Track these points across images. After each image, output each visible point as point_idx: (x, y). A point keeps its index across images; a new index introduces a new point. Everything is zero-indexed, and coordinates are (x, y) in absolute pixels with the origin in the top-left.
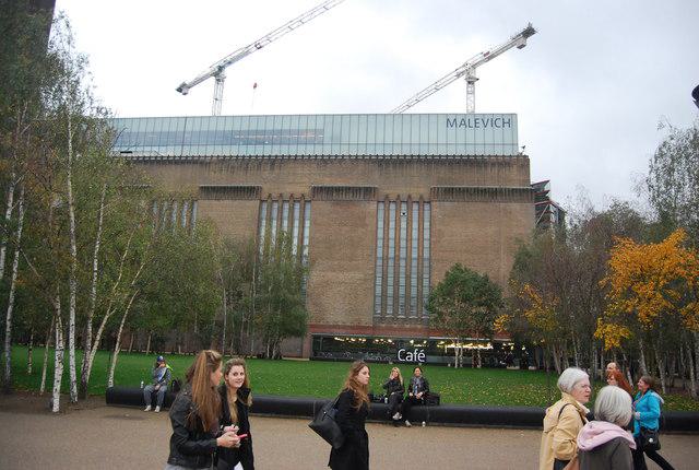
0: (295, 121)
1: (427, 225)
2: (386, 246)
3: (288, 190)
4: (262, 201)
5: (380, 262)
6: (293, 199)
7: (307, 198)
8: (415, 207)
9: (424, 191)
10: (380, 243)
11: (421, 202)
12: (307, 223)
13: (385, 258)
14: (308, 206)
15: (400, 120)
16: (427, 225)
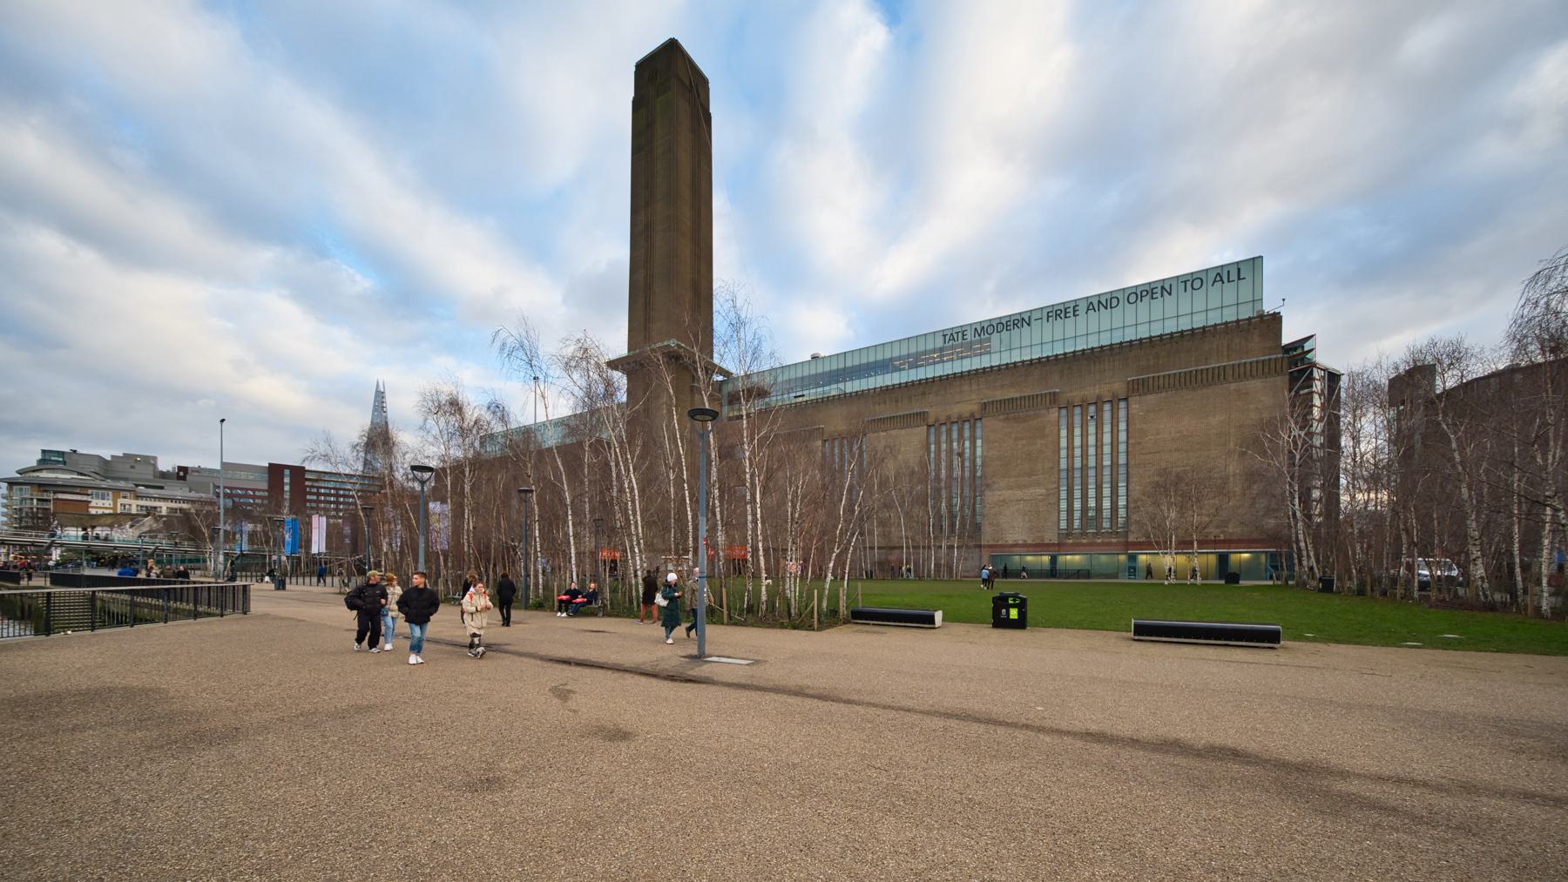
0: (904, 346)
1: (1123, 426)
2: (1070, 456)
3: (956, 410)
4: (929, 426)
5: (1063, 475)
6: (961, 420)
7: (977, 416)
8: (1107, 407)
9: (1119, 387)
10: (1063, 453)
11: (1114, 401)
12: (979, 442)
13: (1070, 469)
14: (979, 424)
15: (923, 340)
16: (1123, 426)
